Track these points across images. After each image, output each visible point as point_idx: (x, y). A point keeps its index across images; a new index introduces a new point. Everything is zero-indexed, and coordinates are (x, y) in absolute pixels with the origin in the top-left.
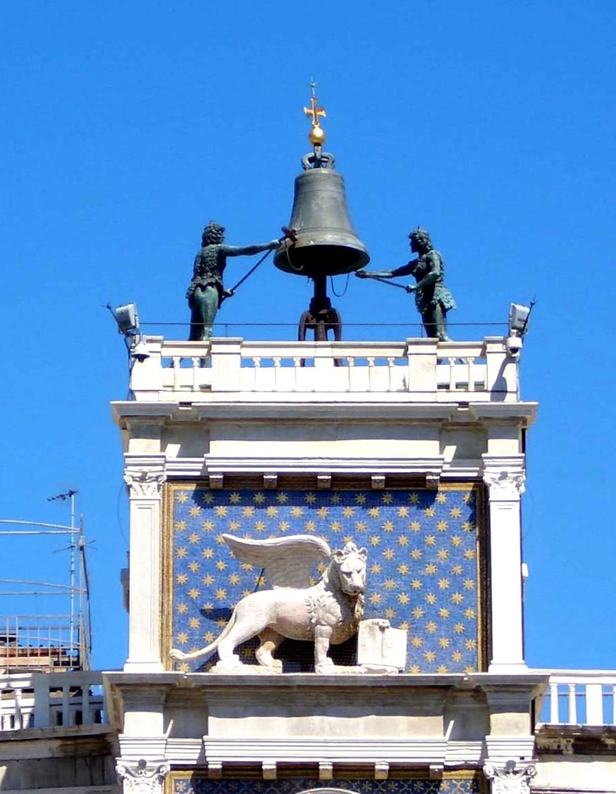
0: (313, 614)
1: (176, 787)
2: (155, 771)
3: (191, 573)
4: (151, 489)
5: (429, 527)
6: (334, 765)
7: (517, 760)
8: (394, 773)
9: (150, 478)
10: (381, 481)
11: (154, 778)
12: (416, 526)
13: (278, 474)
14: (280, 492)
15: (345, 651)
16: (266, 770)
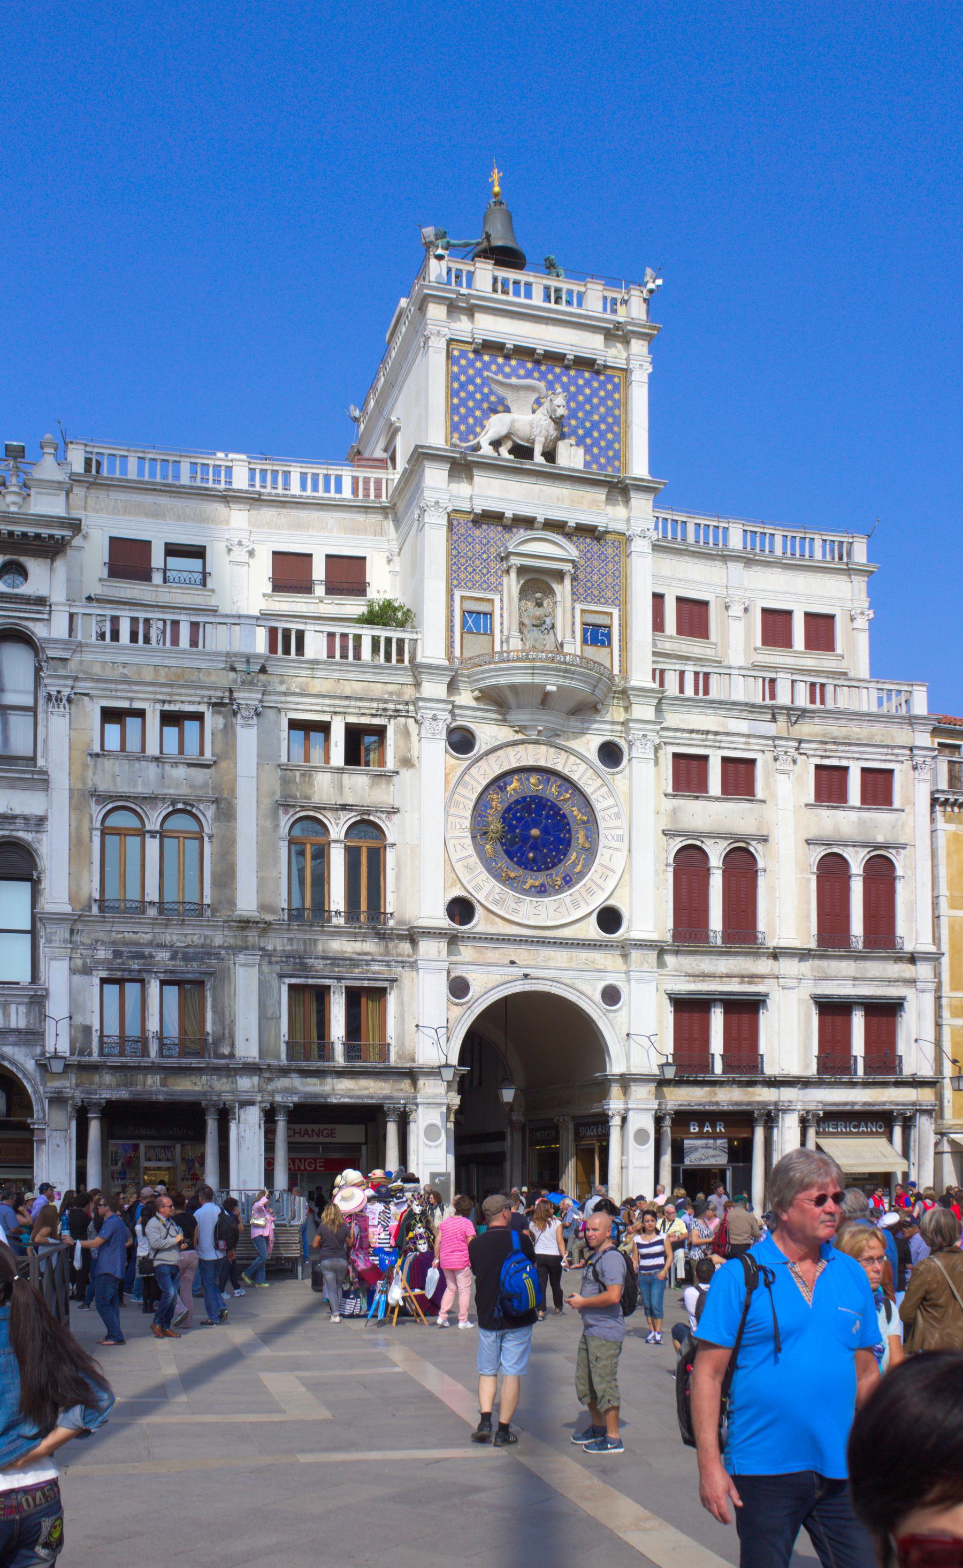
5: (595, 393)
12: (587, 391)
15: (550, 455)
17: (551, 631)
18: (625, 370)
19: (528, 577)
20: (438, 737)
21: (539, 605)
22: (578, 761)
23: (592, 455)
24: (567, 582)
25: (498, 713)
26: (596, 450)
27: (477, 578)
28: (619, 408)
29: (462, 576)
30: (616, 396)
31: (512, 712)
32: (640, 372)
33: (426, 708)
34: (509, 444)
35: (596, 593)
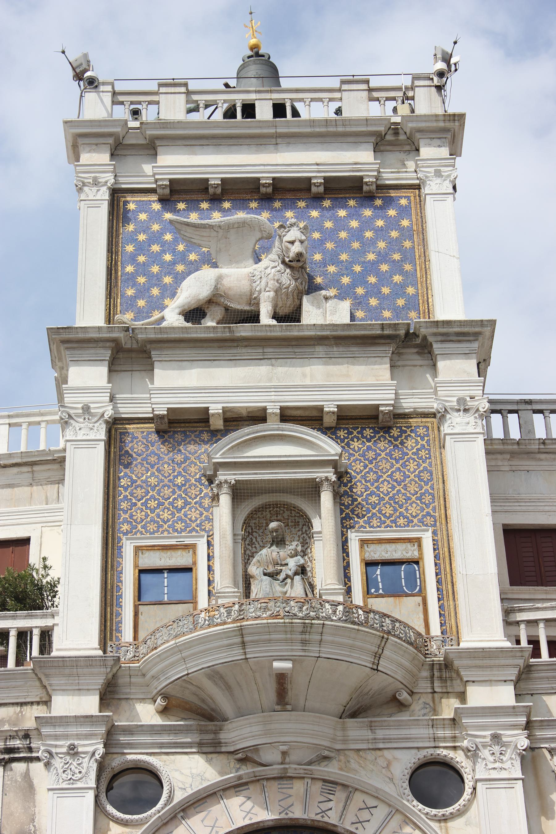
0: (258, 282)
1: (121, 439)
2: (98, 417)
3: (138, 264)
4: (101, 192)
5: (367, 224)
6: (282, 408)
7: (468, 399)
8: (340, 422)
9: (99, 183)
10: (321, 183)
11: (98, 424)
12: (354, 224)
13: (222, 180)
14: (224, 201)
16: (213, 415)
17: (297, 578)
18: (418, 187)
19: (257, 502)
20: (79, 785)
21: (279, 542)
22: (371, 802)
23: (368, 309)
24: (326, 498)
25: (202, 731)
26: (373, 302)
27: (166, 515)
28: (411, 238)
29: (139, 516)
30: (405, 223)
31: (228, 726)
32: (439, 180)
33: (56, 737)
34: (219, 313)
35: (388, 511)
